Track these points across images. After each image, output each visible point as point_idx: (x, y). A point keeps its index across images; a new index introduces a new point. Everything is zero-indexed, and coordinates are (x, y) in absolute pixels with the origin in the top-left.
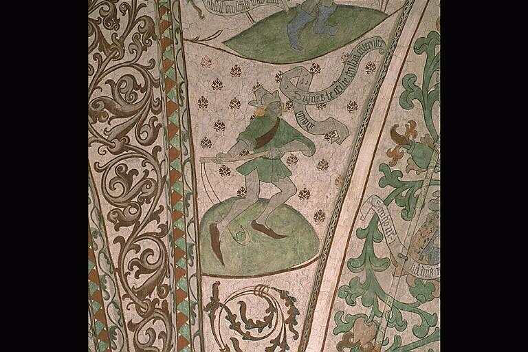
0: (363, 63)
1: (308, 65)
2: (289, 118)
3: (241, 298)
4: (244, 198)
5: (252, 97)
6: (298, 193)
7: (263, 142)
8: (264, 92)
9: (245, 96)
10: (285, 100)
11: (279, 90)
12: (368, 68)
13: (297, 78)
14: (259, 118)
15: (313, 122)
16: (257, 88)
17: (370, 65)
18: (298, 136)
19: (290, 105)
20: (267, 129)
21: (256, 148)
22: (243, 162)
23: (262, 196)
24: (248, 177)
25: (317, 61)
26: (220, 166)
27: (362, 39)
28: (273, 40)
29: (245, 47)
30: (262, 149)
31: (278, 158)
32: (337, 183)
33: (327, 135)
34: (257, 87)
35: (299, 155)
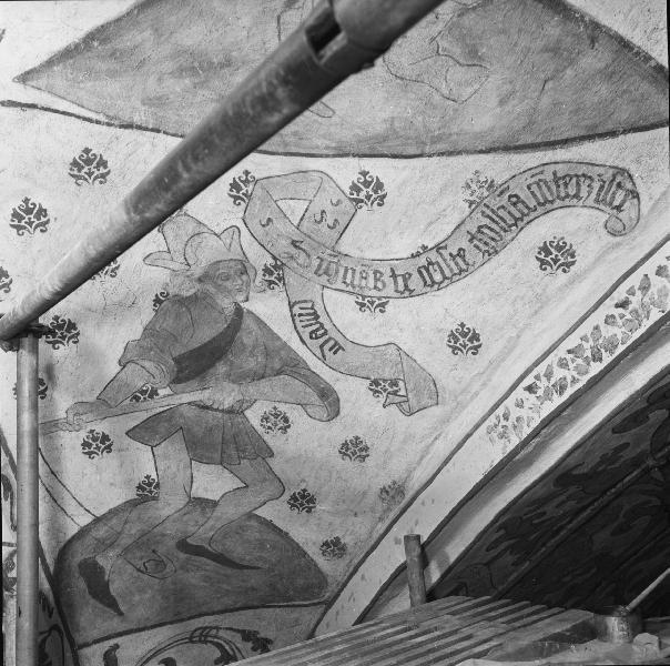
1: (346, 172)
2: (269, 308)
3: (165, 655)
4: (154, 499)
6: (286, 496)
7: (195, 365)
10: (259, 259)
12: (548, 253)
14: (181, 301)
17: (559, 248)
19: (275, 274)
20: (206, 334)
21: (177, 380)
22: (145, 416)
23: (199, 491)
25: (378, 168)
26: (83, 434)
27: (561, 154)
28: (222, 66)
29: (113, 87)
30: (194, 383)
32: (384, 495)
33: (376, 383)
35: (295, 414)
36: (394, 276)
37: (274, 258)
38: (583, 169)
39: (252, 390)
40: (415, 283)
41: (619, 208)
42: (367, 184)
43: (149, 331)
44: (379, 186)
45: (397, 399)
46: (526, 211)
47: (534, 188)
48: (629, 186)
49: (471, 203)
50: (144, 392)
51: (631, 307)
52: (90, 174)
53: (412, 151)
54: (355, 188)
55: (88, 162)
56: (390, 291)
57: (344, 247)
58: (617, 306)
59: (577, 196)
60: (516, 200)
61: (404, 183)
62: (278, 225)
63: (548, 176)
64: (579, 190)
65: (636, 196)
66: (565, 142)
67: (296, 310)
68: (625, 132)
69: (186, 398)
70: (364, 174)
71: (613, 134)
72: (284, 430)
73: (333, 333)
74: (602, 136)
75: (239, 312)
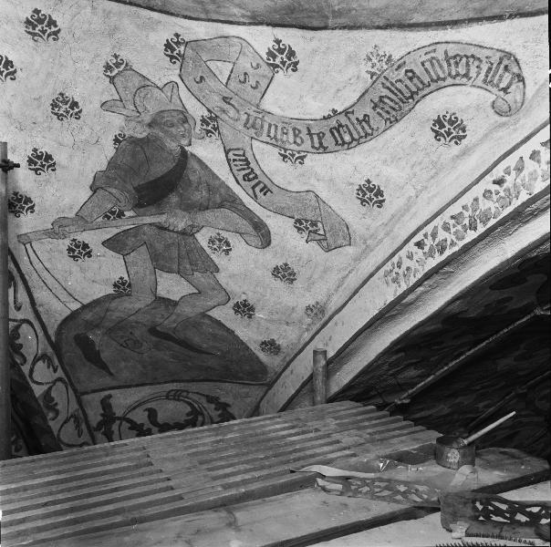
0: (436, 104)
1: (262, 39)
2: (208, 152)
3: (149, 406)
5: (110, 94)
6: (231, 303)
8: (137, 81)
9: (90, 89)
11: (179, 81)
12: (442, 126)
13: (230, 65)
14: (134, 141)
15: (267, 182)
16: (116, 69)
17: (451, 122)
18: (231, 202)
19: (211, 125)
20: (159, 170)
22: (116, 231)
23: (162, 292)
24: (130, 258)
26: (67, 242)
30: (153, 209)
31: (188, 234)
32: (309, 312)
33: (298, 221)
34: (118, 65)
35: (234, 240)
36: (310, 134)
37: (209, 110)
38: (473, 51)
39: (200, 218)
40: (328, 141)
41: (505, 90)
42: (281, 51)
43: (112, 164)
44: (292, 53)
45: (319, 237)
46: (421, 86)
47: (428, 65)
48: (515, 70)
49: (372, 74)
50: (113, 213)
51: (505, 185)
52: (44, 32)
53: (316, 23)
54: (270, 54)
55: (40, 21)
56: (307, 145)
57: (268, 104)
58: (495, 182)
59: (466, 75)
60: (411, 75)
61: (315, 51)
62: (210, 82)
63: (441, 56)
64: (468, 70)
65: (521, 78)
66: (455, 23)
67: (231, 155)
68: (511, 17)
69: (148, 220)
70: (278, 42)
71: (500, 18)
72: (227, 252)
73: (261, 178)
74: (491, 19)
75: (184, 154)
